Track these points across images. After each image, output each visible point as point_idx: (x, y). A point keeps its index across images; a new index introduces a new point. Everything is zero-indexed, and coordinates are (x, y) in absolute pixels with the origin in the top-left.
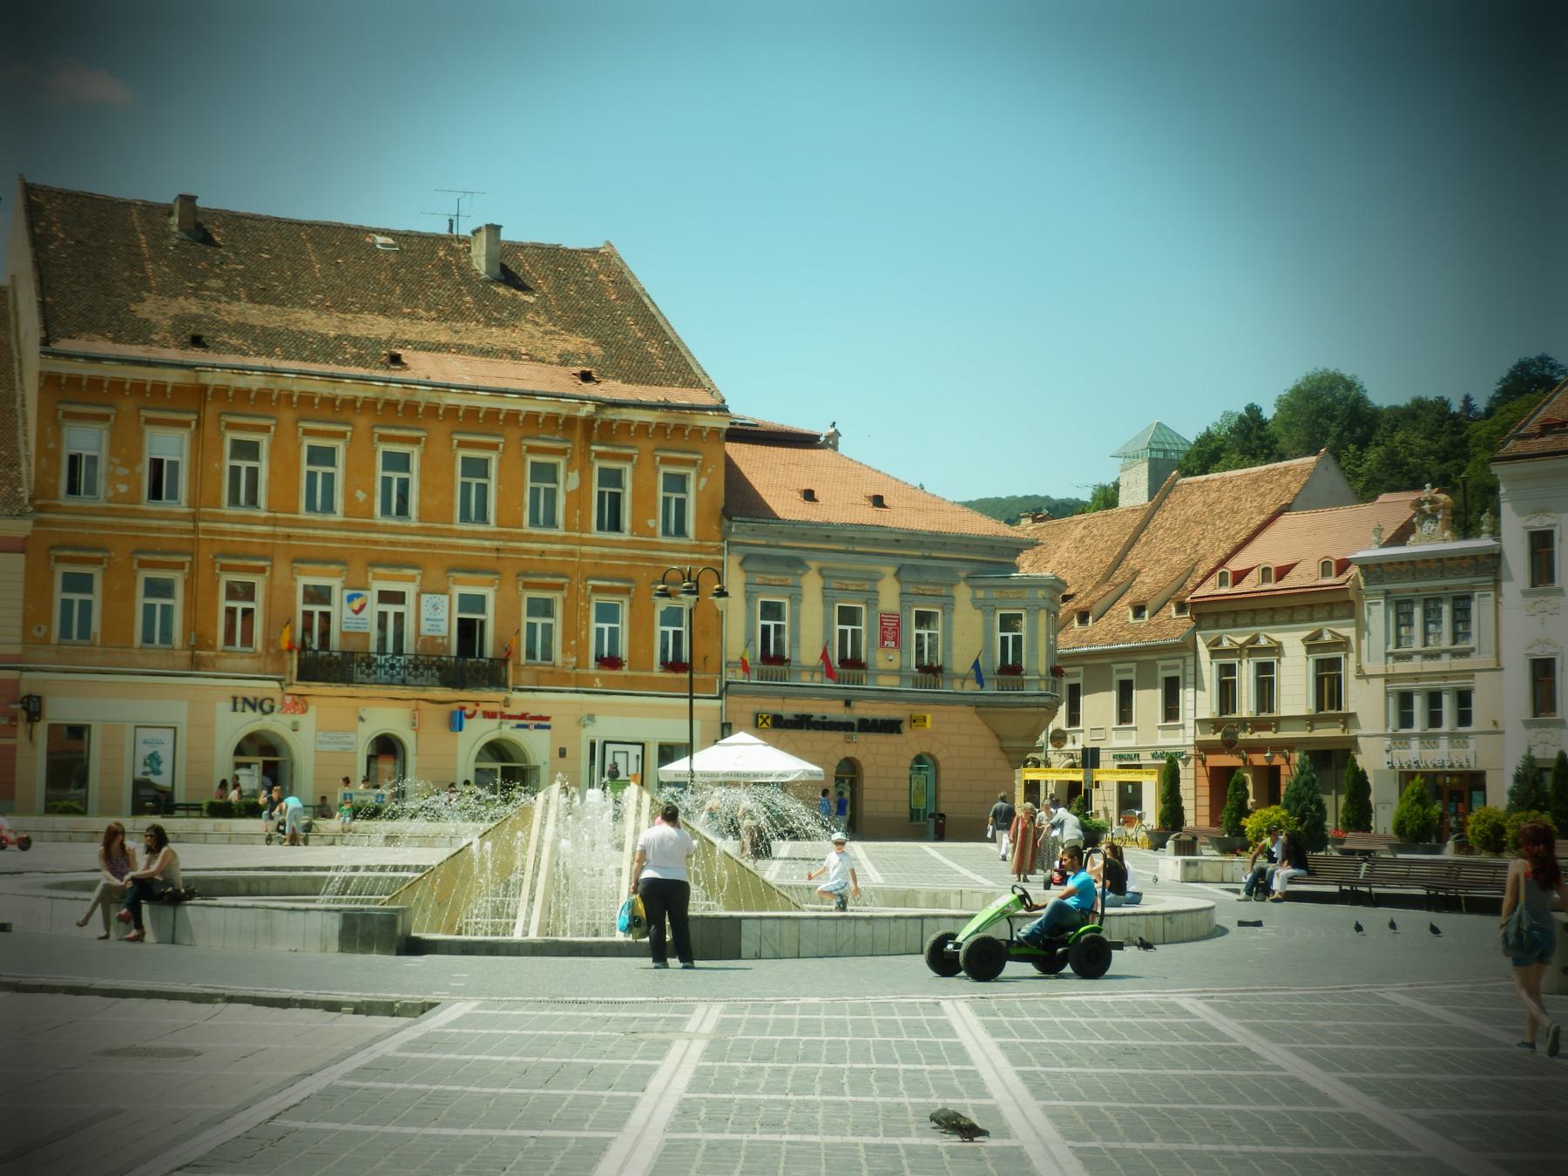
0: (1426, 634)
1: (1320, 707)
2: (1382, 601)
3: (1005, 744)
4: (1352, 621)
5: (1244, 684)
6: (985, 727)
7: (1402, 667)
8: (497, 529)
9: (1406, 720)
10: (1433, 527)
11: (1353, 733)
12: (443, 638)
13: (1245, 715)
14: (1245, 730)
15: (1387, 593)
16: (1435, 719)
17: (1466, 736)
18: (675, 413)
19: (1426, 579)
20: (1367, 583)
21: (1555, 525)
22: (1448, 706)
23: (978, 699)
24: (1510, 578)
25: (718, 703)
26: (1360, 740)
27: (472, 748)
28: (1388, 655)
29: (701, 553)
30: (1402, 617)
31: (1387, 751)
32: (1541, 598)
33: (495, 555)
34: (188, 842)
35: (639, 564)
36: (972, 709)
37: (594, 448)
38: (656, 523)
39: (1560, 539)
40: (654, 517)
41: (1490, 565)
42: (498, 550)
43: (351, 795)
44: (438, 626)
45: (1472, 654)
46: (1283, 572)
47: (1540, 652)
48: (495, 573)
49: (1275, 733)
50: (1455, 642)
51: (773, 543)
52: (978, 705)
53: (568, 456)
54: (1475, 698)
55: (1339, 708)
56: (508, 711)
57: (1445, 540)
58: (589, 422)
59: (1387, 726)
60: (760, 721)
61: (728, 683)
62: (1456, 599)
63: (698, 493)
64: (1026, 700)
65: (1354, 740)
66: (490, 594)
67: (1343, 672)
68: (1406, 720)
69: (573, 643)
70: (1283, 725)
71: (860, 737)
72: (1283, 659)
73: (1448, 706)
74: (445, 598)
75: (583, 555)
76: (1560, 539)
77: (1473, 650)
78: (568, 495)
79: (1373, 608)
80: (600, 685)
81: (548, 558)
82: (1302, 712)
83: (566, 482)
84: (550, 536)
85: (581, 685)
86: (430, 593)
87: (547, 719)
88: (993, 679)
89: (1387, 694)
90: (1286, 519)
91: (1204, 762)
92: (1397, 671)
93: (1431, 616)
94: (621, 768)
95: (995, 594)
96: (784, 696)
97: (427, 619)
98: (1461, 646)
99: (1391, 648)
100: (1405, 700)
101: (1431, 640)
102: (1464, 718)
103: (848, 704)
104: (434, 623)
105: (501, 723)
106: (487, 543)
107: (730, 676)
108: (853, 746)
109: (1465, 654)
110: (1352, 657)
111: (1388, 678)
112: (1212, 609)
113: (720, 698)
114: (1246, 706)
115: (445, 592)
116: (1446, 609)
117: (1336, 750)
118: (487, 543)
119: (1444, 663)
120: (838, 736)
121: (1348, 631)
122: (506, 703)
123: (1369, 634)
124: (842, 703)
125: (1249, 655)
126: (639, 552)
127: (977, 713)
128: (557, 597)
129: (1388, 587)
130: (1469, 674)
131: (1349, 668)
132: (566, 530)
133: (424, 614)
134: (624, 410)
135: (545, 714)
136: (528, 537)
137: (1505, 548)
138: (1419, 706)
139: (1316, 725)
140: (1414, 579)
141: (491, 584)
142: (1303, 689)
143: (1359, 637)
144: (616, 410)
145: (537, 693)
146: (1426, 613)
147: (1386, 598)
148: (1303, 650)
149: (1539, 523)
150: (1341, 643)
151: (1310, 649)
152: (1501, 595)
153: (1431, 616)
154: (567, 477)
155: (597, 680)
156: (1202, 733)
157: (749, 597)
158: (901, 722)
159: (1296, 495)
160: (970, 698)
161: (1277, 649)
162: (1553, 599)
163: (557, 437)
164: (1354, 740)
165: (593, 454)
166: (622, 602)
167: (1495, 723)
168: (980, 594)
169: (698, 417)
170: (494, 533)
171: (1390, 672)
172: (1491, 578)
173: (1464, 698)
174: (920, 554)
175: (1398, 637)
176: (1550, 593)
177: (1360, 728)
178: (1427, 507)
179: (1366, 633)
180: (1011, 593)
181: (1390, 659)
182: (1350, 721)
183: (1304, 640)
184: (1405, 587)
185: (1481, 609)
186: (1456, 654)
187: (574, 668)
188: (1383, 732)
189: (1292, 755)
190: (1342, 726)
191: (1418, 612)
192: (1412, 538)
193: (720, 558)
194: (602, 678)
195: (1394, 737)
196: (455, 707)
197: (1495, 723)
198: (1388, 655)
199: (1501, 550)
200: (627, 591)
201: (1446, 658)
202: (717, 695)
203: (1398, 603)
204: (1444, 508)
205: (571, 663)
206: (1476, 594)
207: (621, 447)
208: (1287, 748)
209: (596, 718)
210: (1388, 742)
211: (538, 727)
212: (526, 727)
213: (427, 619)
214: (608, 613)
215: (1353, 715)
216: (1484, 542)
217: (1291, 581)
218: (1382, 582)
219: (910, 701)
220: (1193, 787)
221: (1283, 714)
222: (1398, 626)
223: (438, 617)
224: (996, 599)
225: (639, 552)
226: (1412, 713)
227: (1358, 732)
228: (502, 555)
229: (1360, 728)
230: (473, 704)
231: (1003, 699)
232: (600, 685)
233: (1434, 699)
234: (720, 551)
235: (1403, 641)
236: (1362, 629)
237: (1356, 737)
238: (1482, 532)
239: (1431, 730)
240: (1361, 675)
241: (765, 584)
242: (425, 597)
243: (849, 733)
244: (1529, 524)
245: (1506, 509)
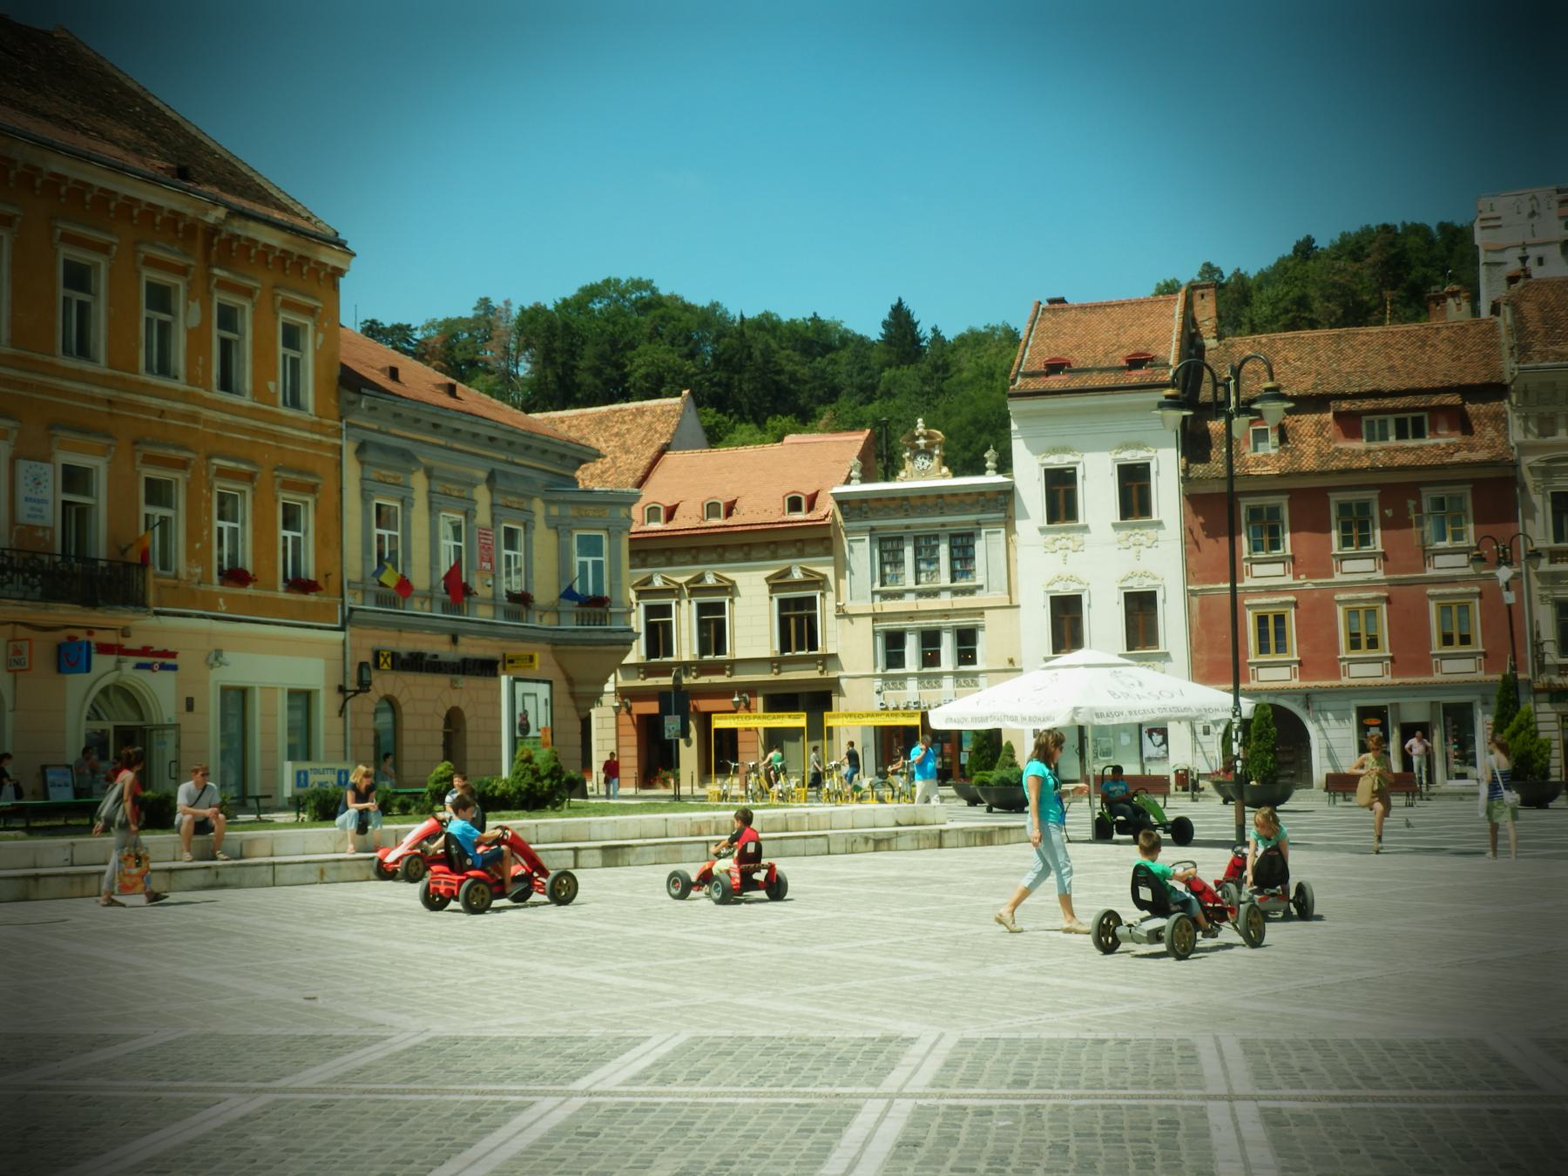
0: (918, 572)
1: (785, 646)
2: (867, 538)
3: (578, 689)
4: (831, 558)
5: (684, 625)
6: (557, 669)
7: (891, 606)
8: (108, 371)
9: (894, 658)
10: (927, 463)
11: (833, 675)
12: (44, 528)
13: (686, 657)
14: (687, 674)
15: (873, 529)
16: (930, 658)
18: (301, 241)
19: (921, 515)
20: (846, 520)
21: (1078, 463)
23: (558, 635)
24: (1026, 516)
25: (340, 636)
26: (843, 682)
27: (85, 699)
28: (874, 593)
29: (321, 434)
30: (885, 555)
31: (878, 693)
32: (1063, 534)
33: (106, 409)
34: (238, 886)
35: (261, 441)
36: (548, 647)
37: (217, 271)
38: (276, 386)
39: (1084, 477)
40: (275, 379)
41: (1002, 502)
42: (110, 402)
43: (306, 773)
44: (40, 511)
45: (978, 592)
46: (730, 508)
47: (1138, 585)
48: (109, 436)
49: (730, 676)
50: (953, 580)
51: (383, 429)
52: (554, 643)
53: (190, 278)
54: (981, 636)
55: (813, 646)
56: (129, 644)
57: (944, 476)
58: (213, 231)
59: (875, 666)
60: (382, 660)
61: (351, 610)
62: (953, 537)
63: (316, 352)
64: (613, 636)
65: (836, 681)
66: (98, 465)
67: (673, 619)
68: (894, 658)
69: (198, 546)
70: (737, 668)
71: (464, 681)
72: (737, 599)
74: (47, 468)
75: (207, 423)
76: (1084, 477)
77: (980, 587)
78: (190, 332)
79: (855, 546)
80: (224, 608)
81: (168, 421)
82: (767, 654)
83: (186, 315)
84: (167, 389)
85: (204, 606)
86: (29, 459)
87: (173, 655)
88: (571, 612)
89: (875, 633)
90: (669, 456)
91: (629, 711)
92: (920, 608)
93: (925, 553)
94: (531, 719)
95: (571, 511)
96: (400, 628)
97: (27, 499)
98: (962, 583)
99: (877, 586)
101: (923, 578)
102: (966, 654)
103: (454, 640)
104: (34, 505)
105: (119, 661)
106: (98, 391)
107: (352, 601)
108: (376, 699)
109: (970, 591)
110: (831, 596)
111: (876, 617)
112: (661, 545)
113: (342, 629)
114: (686, 645)
115: (46, 458)
116: (944, 550)
117: (803, 693)
118: (98, 391)
119: (945, 601)
120: (442, 680)
121: (829, 571)
122: (125, 633)
123: (852, 573)
124: (446, 638)
125: (691, 595)
126: (261, 425)
127: (553, 652)
128: (179, 477)
129: (874, 523)
130: (979, 612)
131: (826, 609)
132: (188, 384)
133: (23, 490)
134: (252, 224)
135: (171, 649)
136: (144, 388)
137: (1018, 485)
139: (783, 668)
140: (907, 516)
141: (104, 452)
142: (737, 632)
143: (839, 575)
144: (243, 222)
145: (162, 618)
146: (917, 551)
147: (871, 536)
148: (766, 588)
149: (1058, 461)
150: (725, 588)
151: (774, 588)
152: (1014, 532)
153: (925, 553)
154: (187, 307)
155: (221, 601)
156: (625, 678)
157: (365, 496)
158: (497, 662)
159: (673, 435)
160: (550, 634)
161: (730, 589)
162: (1077, 536)
163: (176, 248)
164: (836, 681)
165: (215, 281)
166: (243, 492)
167: (1011, 661)
168: (554, 510)
169: (323, 249)
170: (105, 377)
171: (878, 611)
172: (1002, 515)
174: (504, 457)
175: (883, 576)
176: (1073, 529)
177: (842, 670)
178: (922, 442)
179: (848, 573)
180: (591, 510)
181: (877, 597)
182: (829, 664)
183: (767, 579)
184: (896, 523)
185: (988, 548)
186: (957, 592)
187: (199, 583)
188: (871, 673)
189: (752, 700)
190: (820, 668)
191: (909, 552)
192: (902, 474)
193: (338, 442)
194: (226, 596)
195: (885, 678)
196: (61, 636)
197: (1011, 661)
198: (874, 593)
199: (1013, 487)
200: (250, 478)
201: (910, 598)
202: (338, 625)
203: (882, 540)
204: (940, 443)
205: (196, 574)
206: (983, 531)
207: (243, 276)
208: (747, 692)
209: (227, 656)
210: (878, 683)
211: (163, 667)
212: (148, 667)
213: (27, 499)
214: (227, 506)
215: (834, 656)
216: (991, 478)
217: (681, 522)
218: (867, 518)
219: (504, 637)
220: (614, 736)
221: (739, 655)
222: (883, 564)
223: (40, 496)
224: (575, 517)
225: (261, 425)
226: (903, 654)
227: (840, 673)
228: (115, 411)
229: (842, 670)
230: (84, 631)
231: (587, 636)
232: (224, 608)
233: (930, 639)
234: (338, 433)
235: (888, 580)
236: (842, 567)
237: (838, 678)
238: (986, 469)
239: (926, 670)
240: (842, 614)
241: (380, 481)
242: (23, 466)
243: (455, 676)
244: (1047, 461)
245: (1018, 447)
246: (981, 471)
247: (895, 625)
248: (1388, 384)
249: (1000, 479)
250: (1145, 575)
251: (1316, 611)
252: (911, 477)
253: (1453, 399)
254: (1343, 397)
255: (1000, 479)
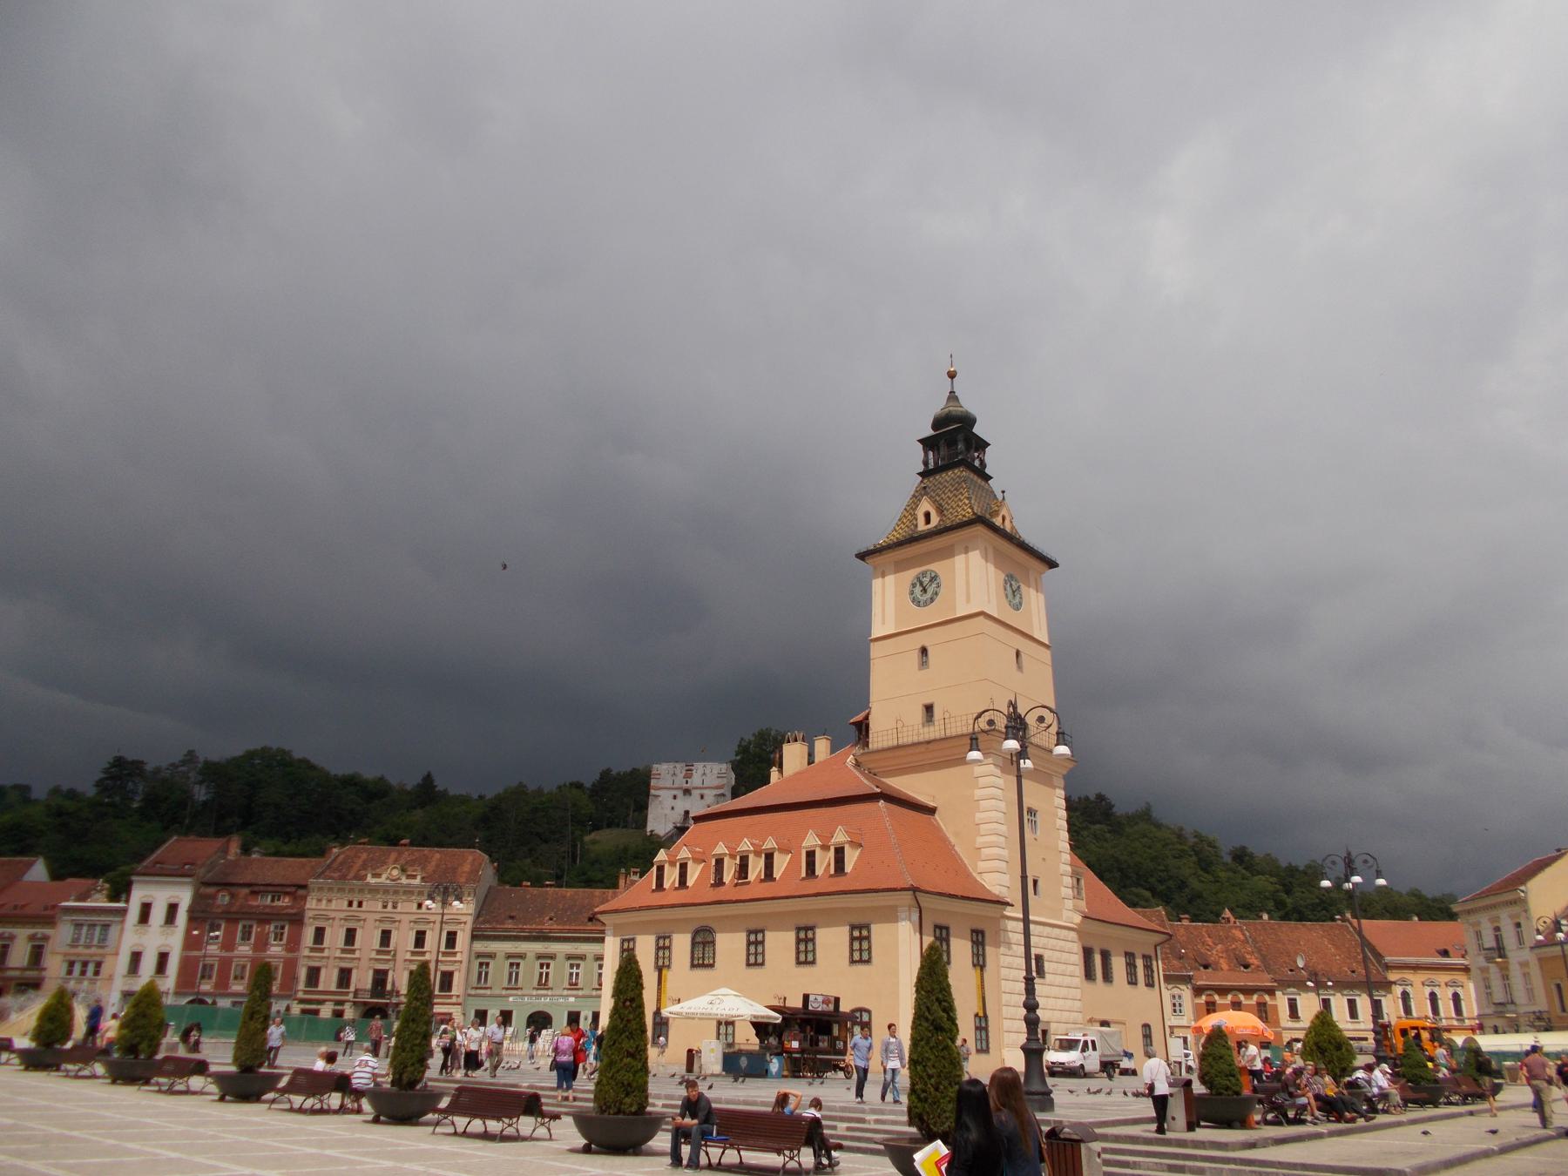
9: (70, 972)
16: (83, 973)
17: (97, 980)
22: (91, 968)
41: (123, 912)
54: (103, 965)
57: (105, 902)
68: (70, 972)
73: (91, 968)
100: (72, 964)
102: (97, 973)
111: (66, 955)
119: (93, 950)
130: (103, 955)
138: (77, 968)
173: (99, 965)
184: (82, 918)
185: (113, 931)
246: (118, 901)
247: (73, 958)
248: (277, 881)
249: (124, 905)
250: (168, 945)
251: (225, 964)
252: (91, 902)
253: (293, 889)
254: (257, 885)
255: (124, 905)
